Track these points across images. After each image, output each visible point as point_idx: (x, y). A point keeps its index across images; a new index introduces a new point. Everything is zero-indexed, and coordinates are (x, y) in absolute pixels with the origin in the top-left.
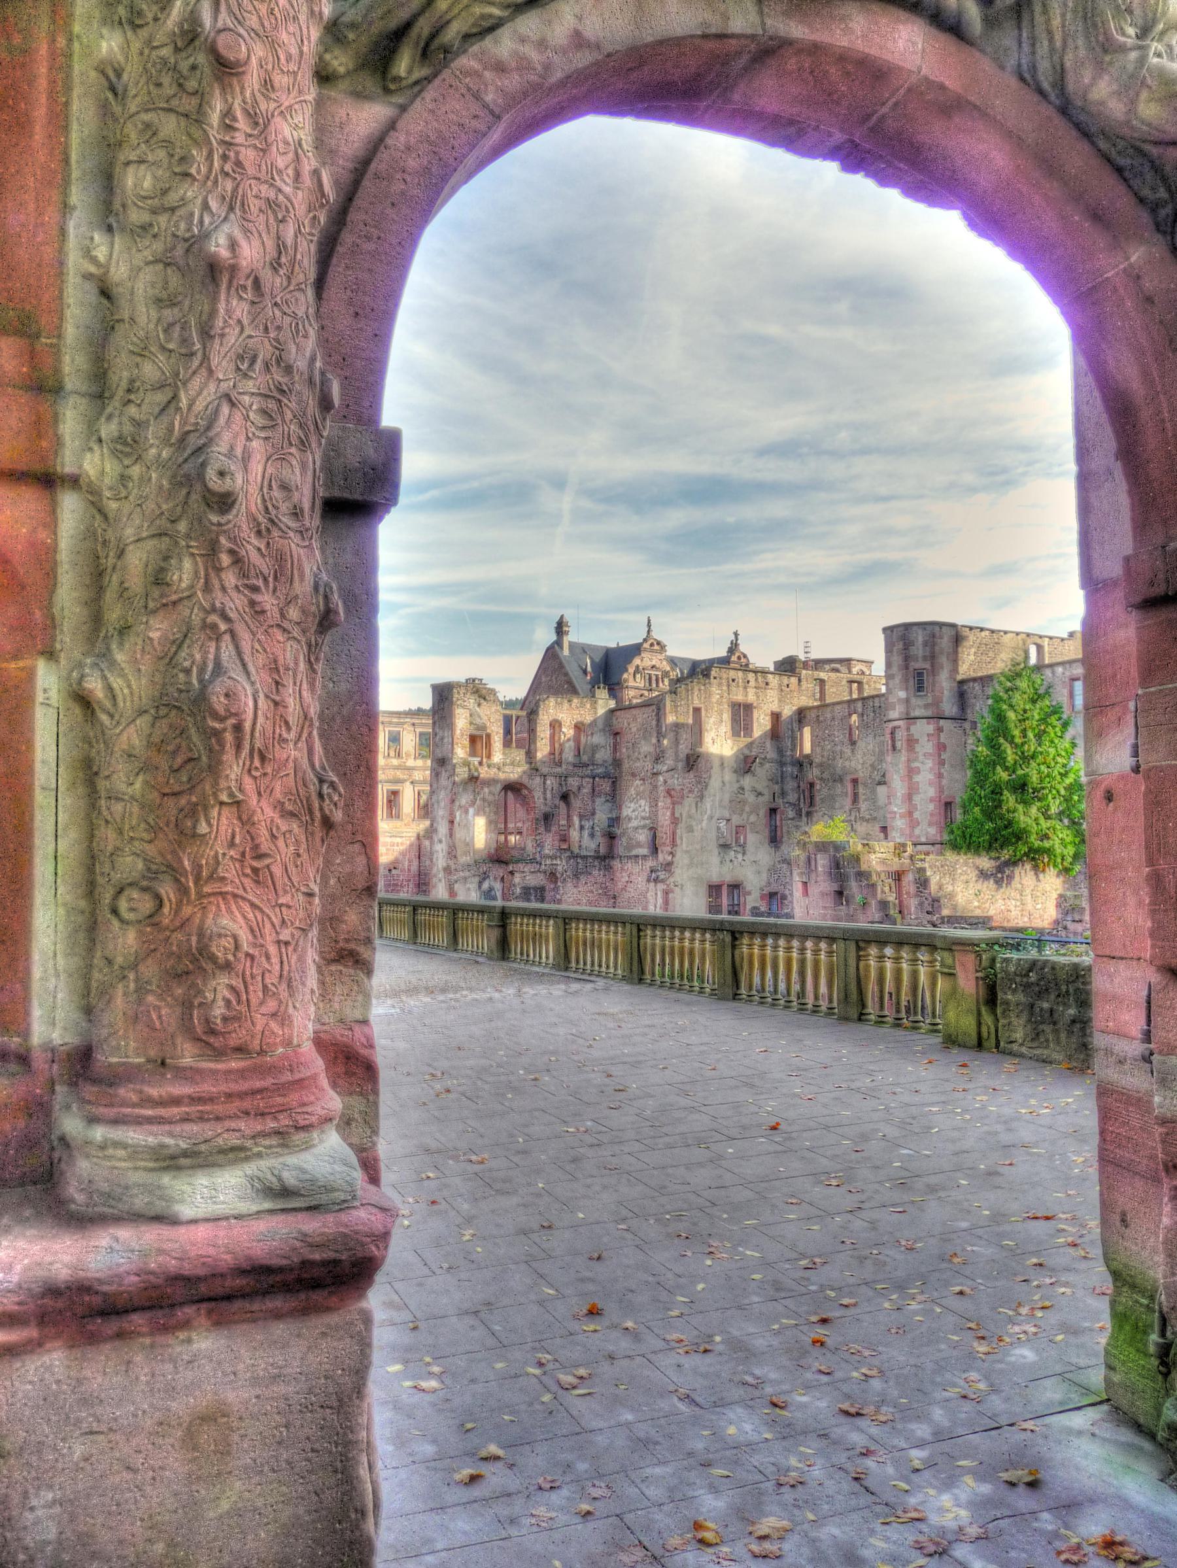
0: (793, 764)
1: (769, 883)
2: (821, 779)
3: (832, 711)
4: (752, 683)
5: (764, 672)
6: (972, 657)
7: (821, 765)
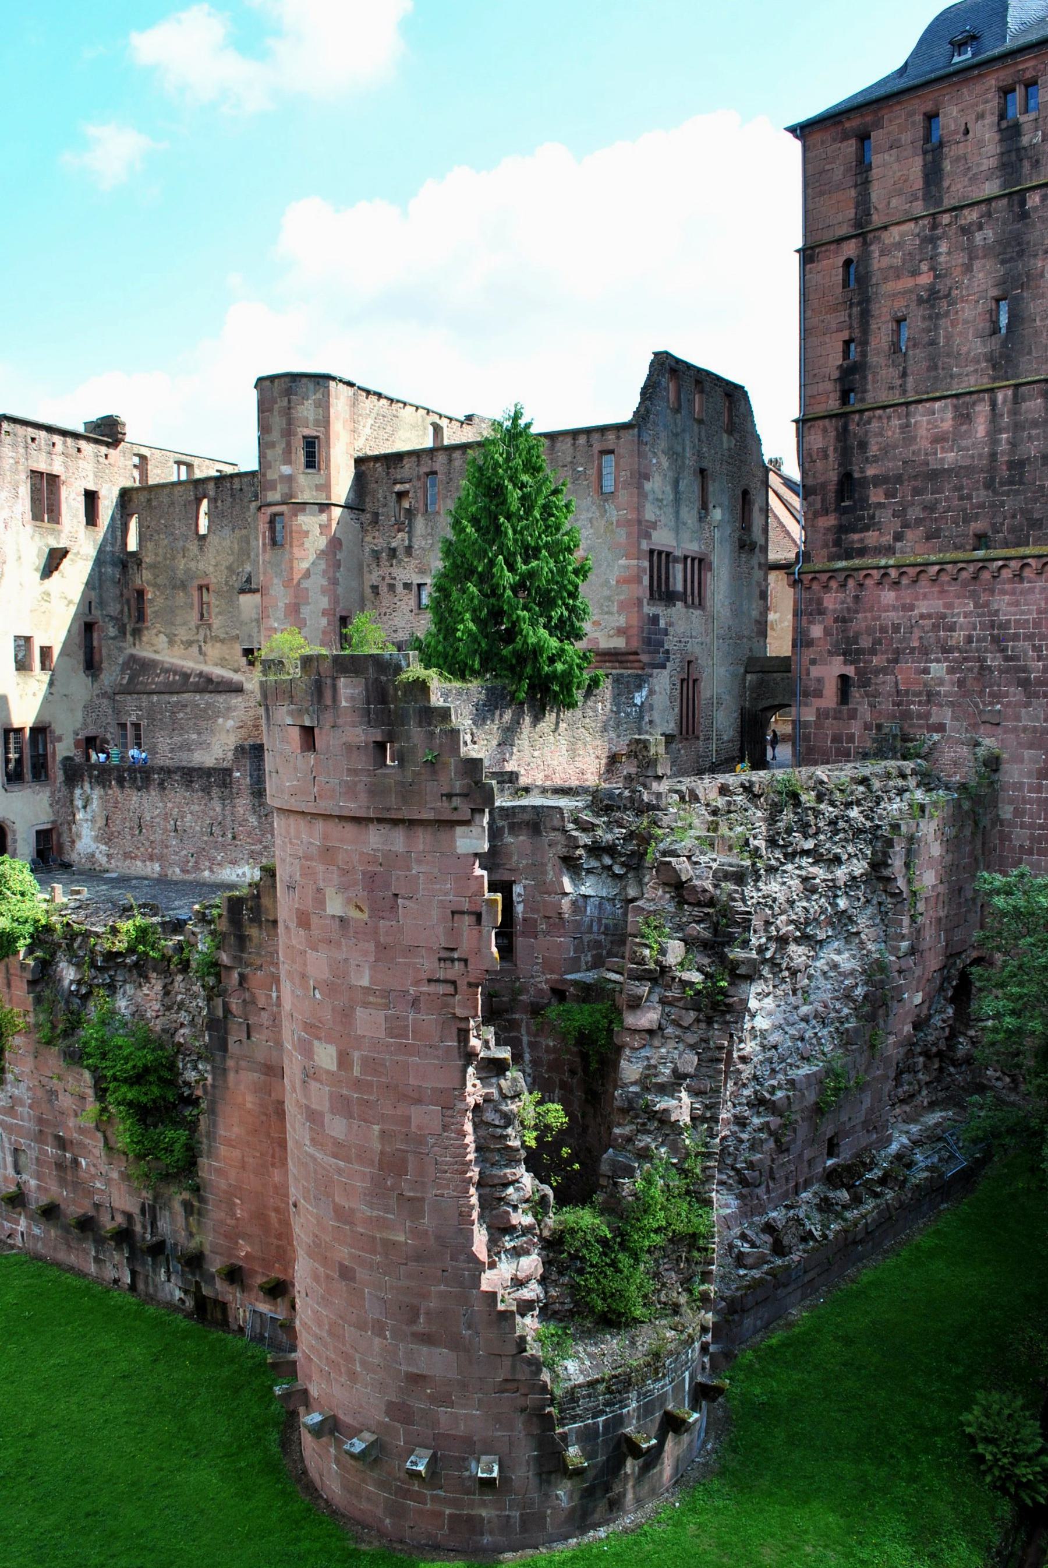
0: (114, 565)
1: (85, 724)
2: (155, 585)
3: (171, 494)
4: (59, 447)
5: (76, 436)
6: (368, 431)
7: (153, 566)
